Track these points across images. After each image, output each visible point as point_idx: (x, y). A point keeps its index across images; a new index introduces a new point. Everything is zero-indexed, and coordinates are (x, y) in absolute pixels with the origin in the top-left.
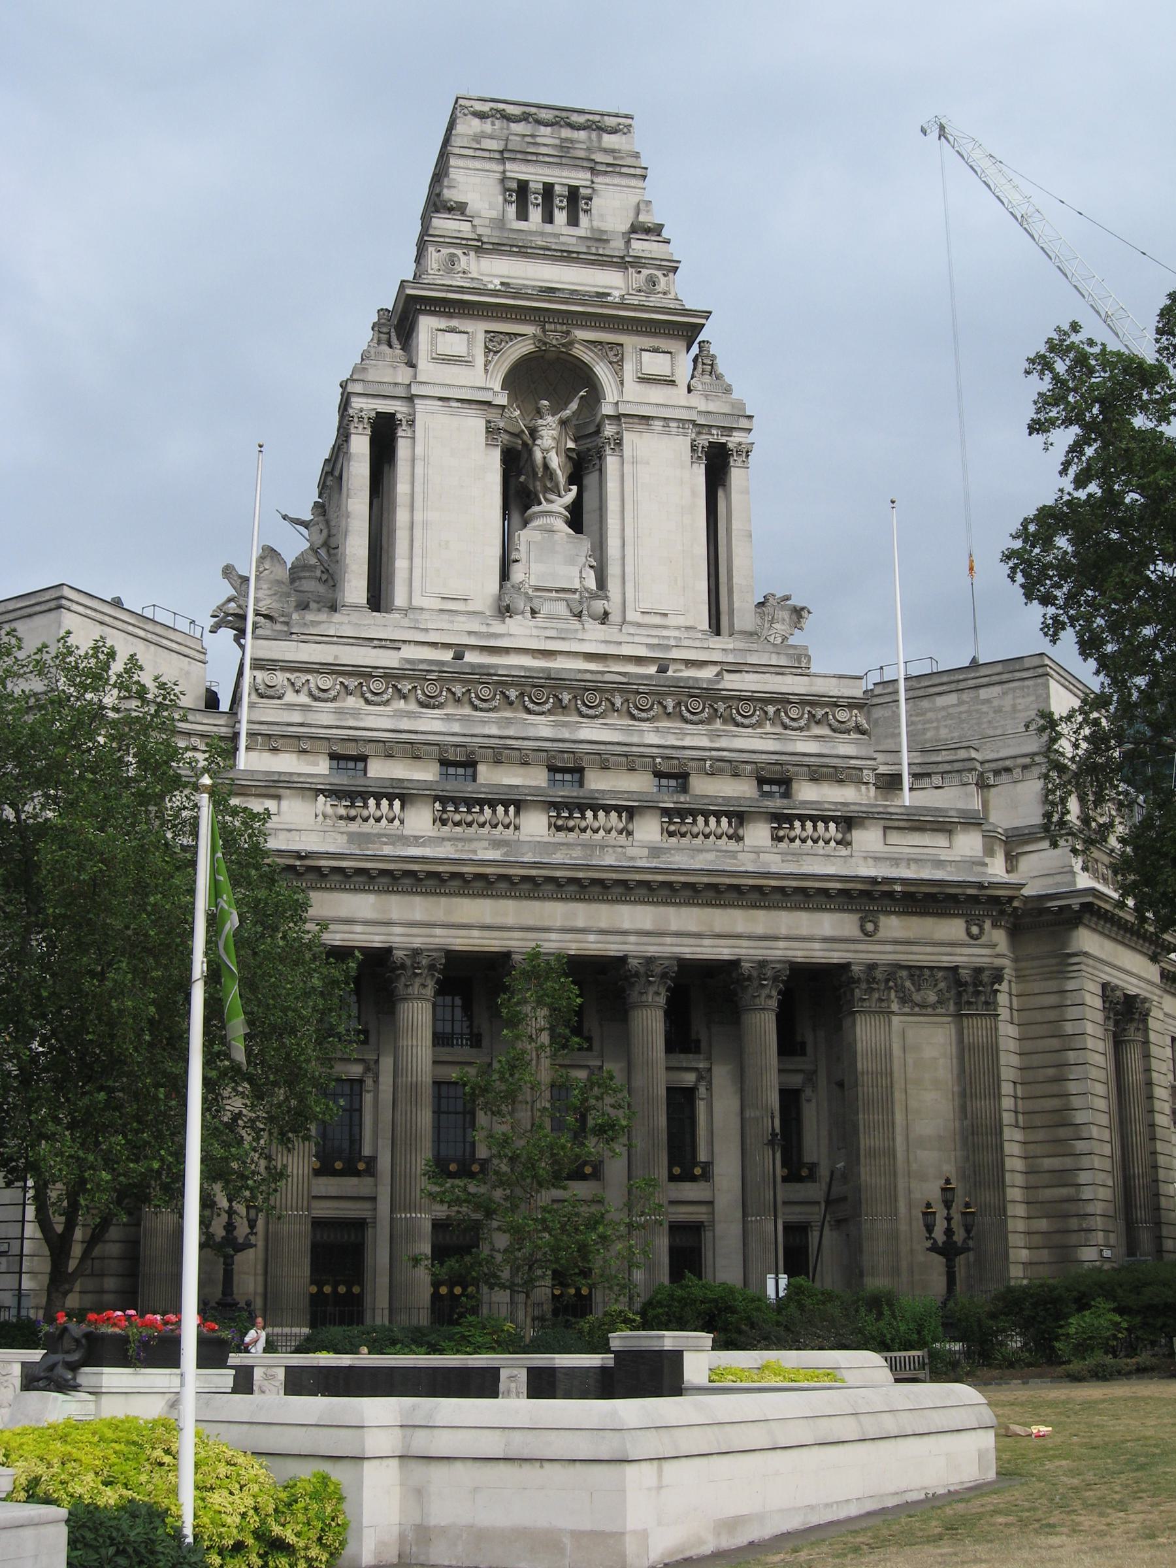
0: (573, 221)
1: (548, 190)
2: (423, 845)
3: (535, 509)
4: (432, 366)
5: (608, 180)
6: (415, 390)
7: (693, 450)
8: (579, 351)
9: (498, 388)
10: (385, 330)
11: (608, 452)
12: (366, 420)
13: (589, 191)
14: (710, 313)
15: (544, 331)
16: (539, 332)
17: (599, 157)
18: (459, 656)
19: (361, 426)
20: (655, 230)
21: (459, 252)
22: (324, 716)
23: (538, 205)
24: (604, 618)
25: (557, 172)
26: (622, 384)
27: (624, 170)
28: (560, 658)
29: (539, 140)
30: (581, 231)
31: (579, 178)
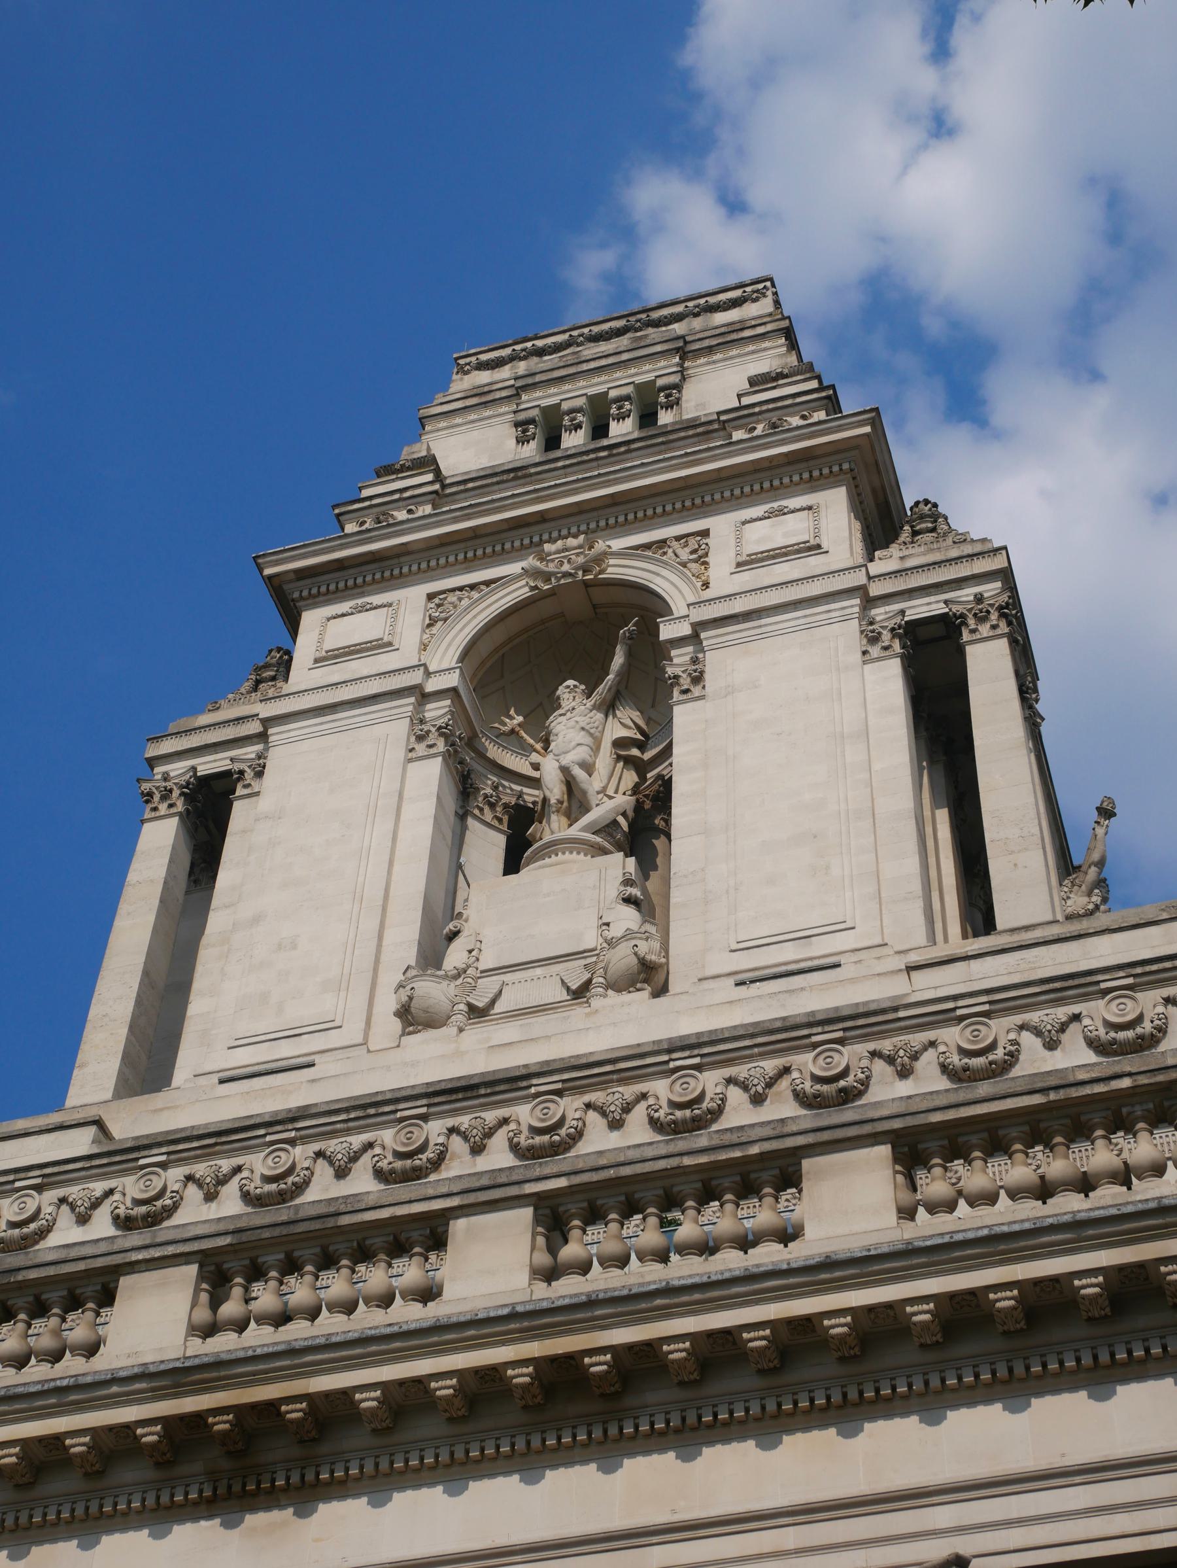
8: (615, 570)
31: (660, 371)
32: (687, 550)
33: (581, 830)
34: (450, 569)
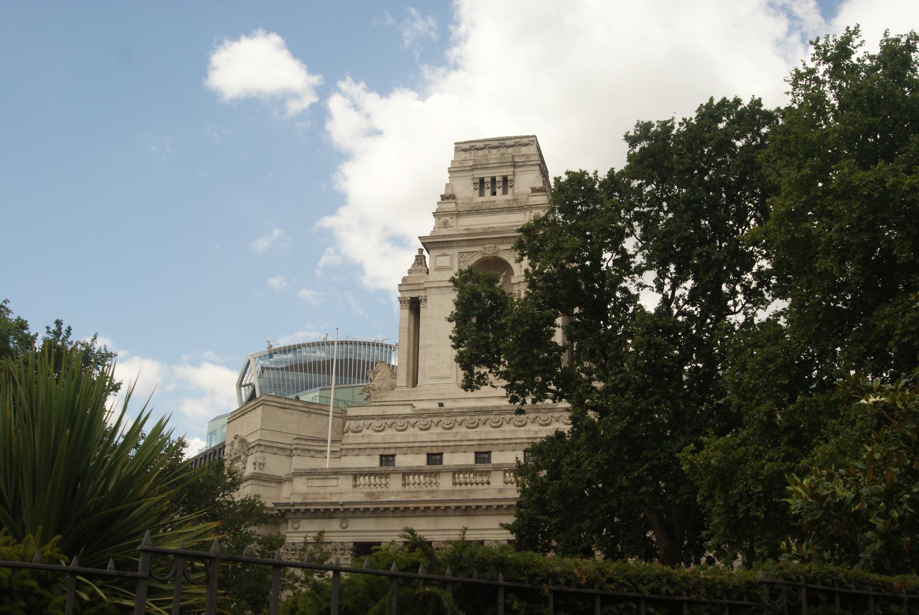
0: (505, 192)
1: (493, 180)
2: (397, 495)
4: (435, 273)
5: (522, 169)
17: (517, 160)
18: (441, 405)
21: (448, 218)
22: (378, 438)
25: (497, 171)
28: (488, 400)
30: (509, 197)
31: (508, 171)
34: (463, 246)
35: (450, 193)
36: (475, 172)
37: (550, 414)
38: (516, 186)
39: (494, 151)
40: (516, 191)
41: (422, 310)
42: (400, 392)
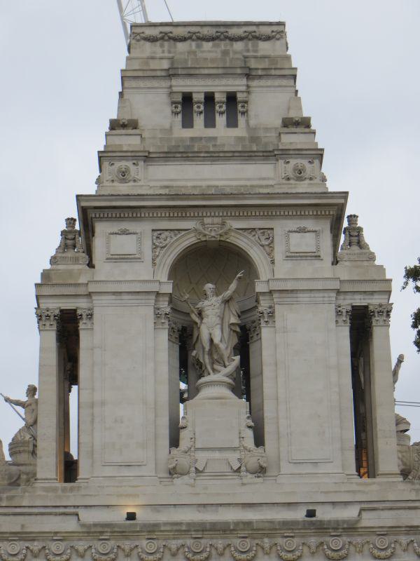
0: (232, 123)
1: (209, 98)
3: (203, 380)
5: (262, 82)
6: (92, 288)
7: (339, 313)
9: (163, 275)
10: (70, 236)
11: (263, 324)
12: (52, 318)
13: (245, 94)
14: (347, 193)
15: (203, 224)
16: (200, 227)
17: (253, 64)
19: (48, 323)
20: (305, 123)
21: (129, 164)
23: (201, 113)
24: (261, 471)
25: (217, 82)
26: (273, 262)
27: (278, 72)
29: (199, 55)
30: (240, 131)
31: (237, 85)
32: (265, 237)
33: (224, 376)
35: (126, 117)
36: (174, 82)
37: (346, 539)
38: (251, 113)
39: (207, 46)
40: (252, 122)
41: (82, 335)
42: (46, 490)
